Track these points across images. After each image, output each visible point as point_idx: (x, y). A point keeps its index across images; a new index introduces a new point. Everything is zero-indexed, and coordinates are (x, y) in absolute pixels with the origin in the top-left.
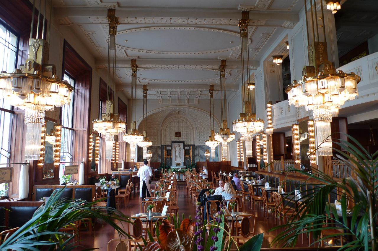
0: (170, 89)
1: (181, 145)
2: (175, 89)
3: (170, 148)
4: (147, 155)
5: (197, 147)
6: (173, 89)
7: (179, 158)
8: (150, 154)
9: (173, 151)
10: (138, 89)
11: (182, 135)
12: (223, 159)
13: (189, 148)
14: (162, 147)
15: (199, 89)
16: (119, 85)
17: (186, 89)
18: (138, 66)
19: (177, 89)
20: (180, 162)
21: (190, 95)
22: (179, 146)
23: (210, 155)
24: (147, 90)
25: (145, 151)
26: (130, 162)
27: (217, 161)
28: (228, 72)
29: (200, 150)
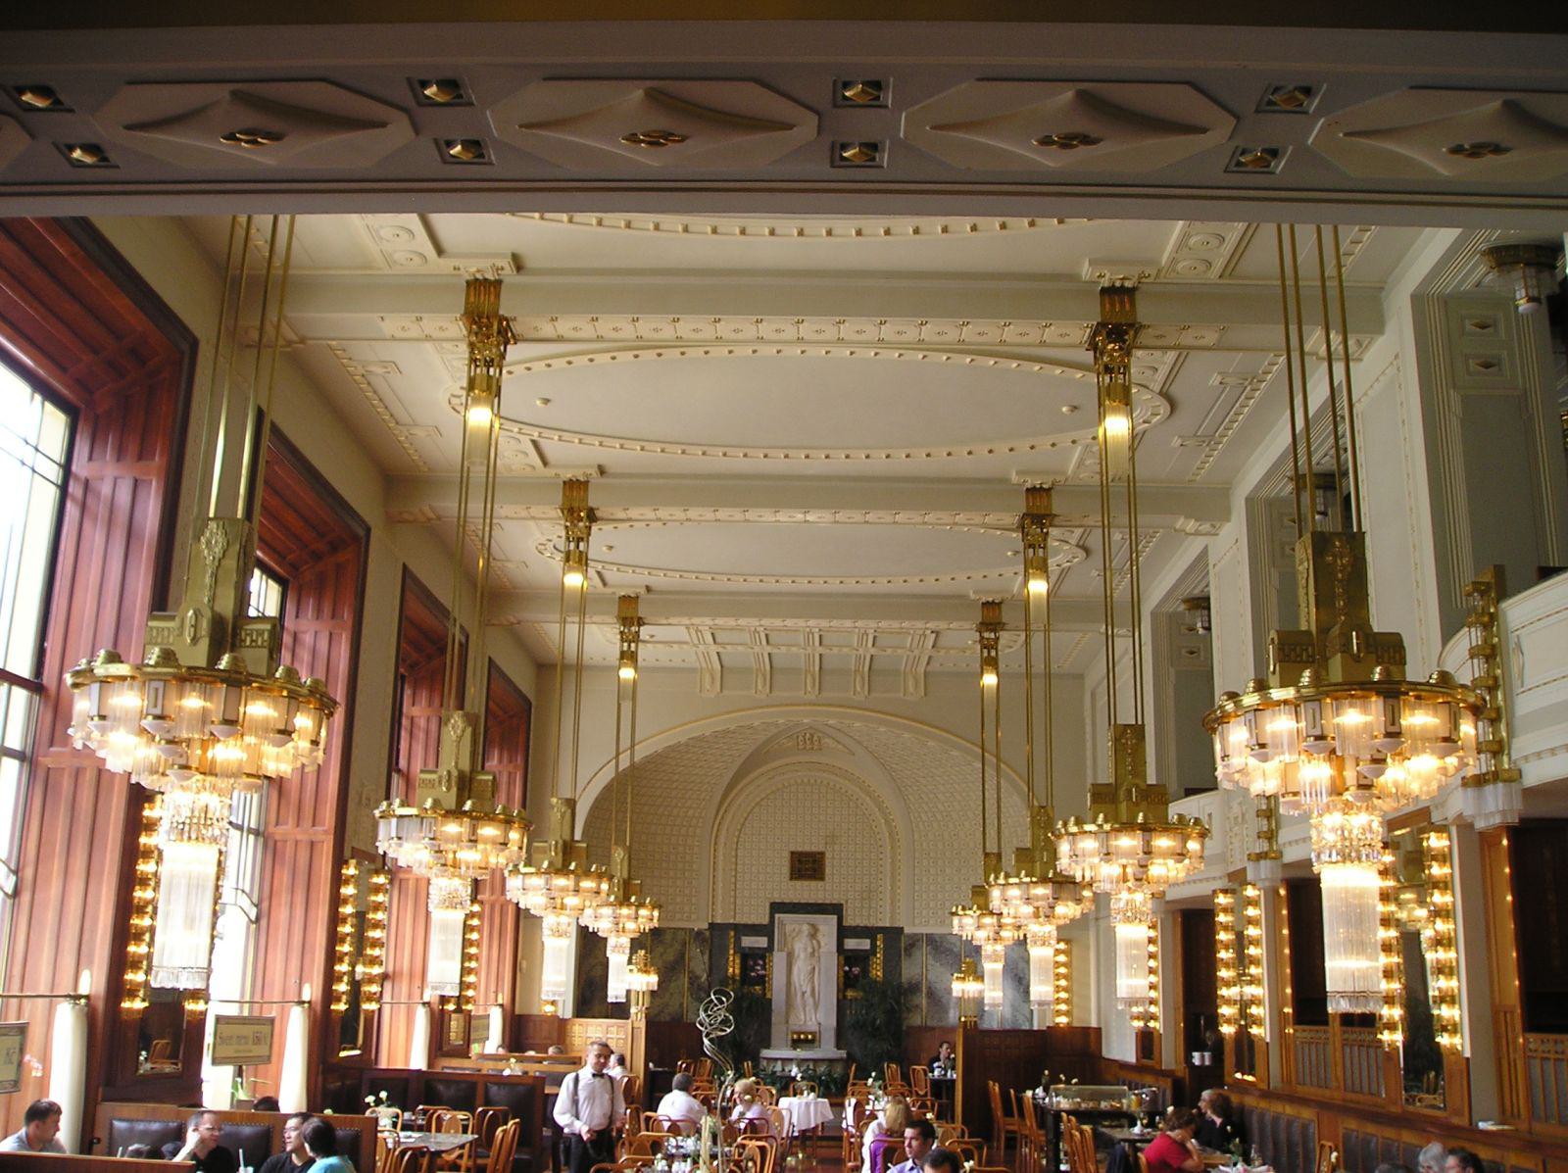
0: (766, 622)
1: (821, 928)
2: (790, 623)
3: (762, 942)
4: (627, 979)
5: (914, 941)
6: (778, 623)
7: (810, 1001)
8: (646, 972)
9: (778, 959)
10: (594, 619)
11: (828, 870)
12: (1059, 1013)
13: (865, 944)
14: (717, 935)
15: (920, 624)
16: (496, 596)
17: (848, 623)
18: (598, 514)
19: (801, 623)
20: (812, 1026)
21: (873, 651)
22: (814, 934)
23: (983, 991)
24: (641, 622)
25: (617, 958)
26: (535, 1012)
27: (1026, 1027)
28: (1073, 542)
29: (931, 961)
